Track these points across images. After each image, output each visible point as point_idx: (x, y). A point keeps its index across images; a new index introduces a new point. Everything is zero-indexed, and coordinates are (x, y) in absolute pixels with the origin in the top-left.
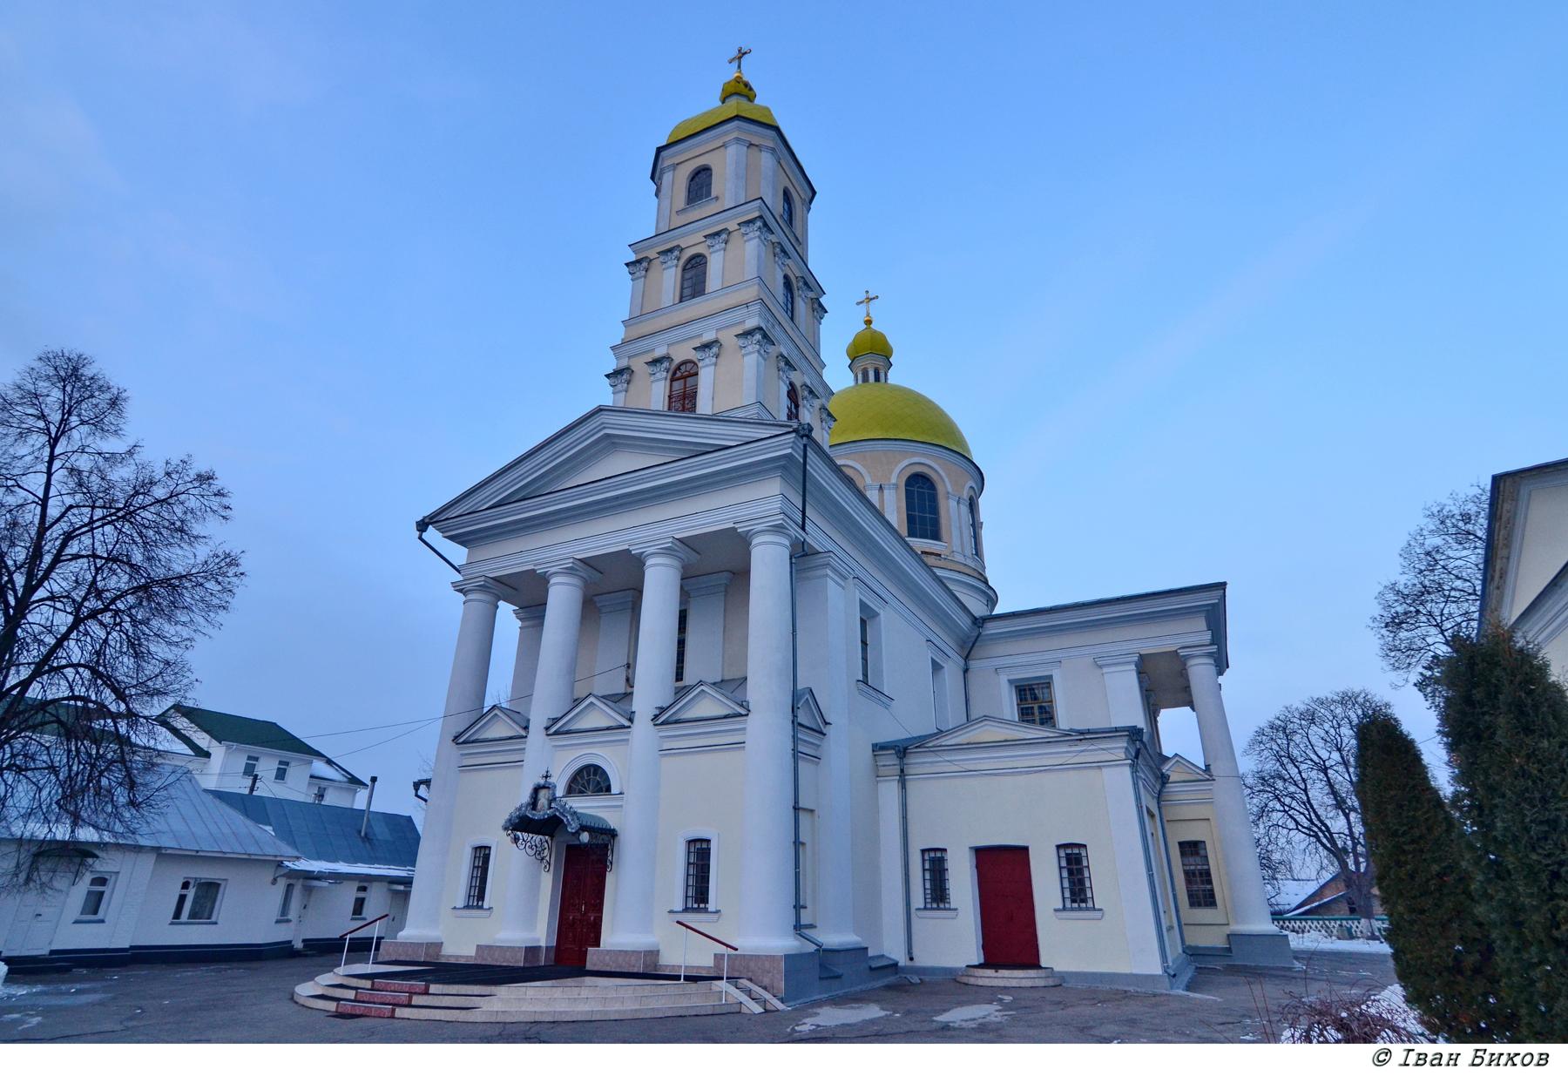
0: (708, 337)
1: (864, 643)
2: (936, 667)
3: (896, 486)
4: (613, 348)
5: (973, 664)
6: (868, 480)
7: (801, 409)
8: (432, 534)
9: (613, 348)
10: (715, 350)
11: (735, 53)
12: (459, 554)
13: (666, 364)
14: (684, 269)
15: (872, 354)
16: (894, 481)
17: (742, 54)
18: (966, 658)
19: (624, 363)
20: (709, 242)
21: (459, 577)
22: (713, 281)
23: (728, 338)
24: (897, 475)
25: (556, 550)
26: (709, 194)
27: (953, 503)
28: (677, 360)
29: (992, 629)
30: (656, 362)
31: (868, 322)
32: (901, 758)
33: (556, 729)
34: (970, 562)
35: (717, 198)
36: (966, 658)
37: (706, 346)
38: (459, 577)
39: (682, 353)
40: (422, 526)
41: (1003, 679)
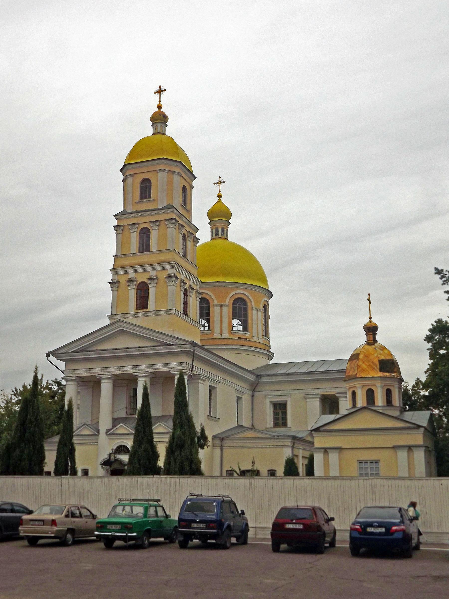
0: (153, 273)
1: (210, 399)
2: (239, 399)
3: (228, 306)
4: (111, 270)
5: (256, 394)
6: (216, 302)
7: (188, 297)
8: (52, 358)
9: (111, 270)
10: (156, 281)
11: (157, 89)
12: (62, 365)
13: (135, 283)
14: (140, 234)
15: (220, 217)
16: (227, 303)
17: (160, 91)
18: (254, 391)
19: (116, 277)
20: (151, 224)
21: (63, 375)
22: (154, 246)
23: (162, 275)
24: (229, 301)
25: (104, 370)
26: (150, 197)
27: (254, 312)
28: (140, 280)
29: (264, 380)
30: (130, 281)
31: (219, 197)
32: (221, 441)
33: (108, 433)
34: (261, 341)
35: (154, 200)
36: (254, 391)
37: (152, 279)
38: (63, 375)
39: (142, 278)
40: (48, 355)
41: (268, 400)
